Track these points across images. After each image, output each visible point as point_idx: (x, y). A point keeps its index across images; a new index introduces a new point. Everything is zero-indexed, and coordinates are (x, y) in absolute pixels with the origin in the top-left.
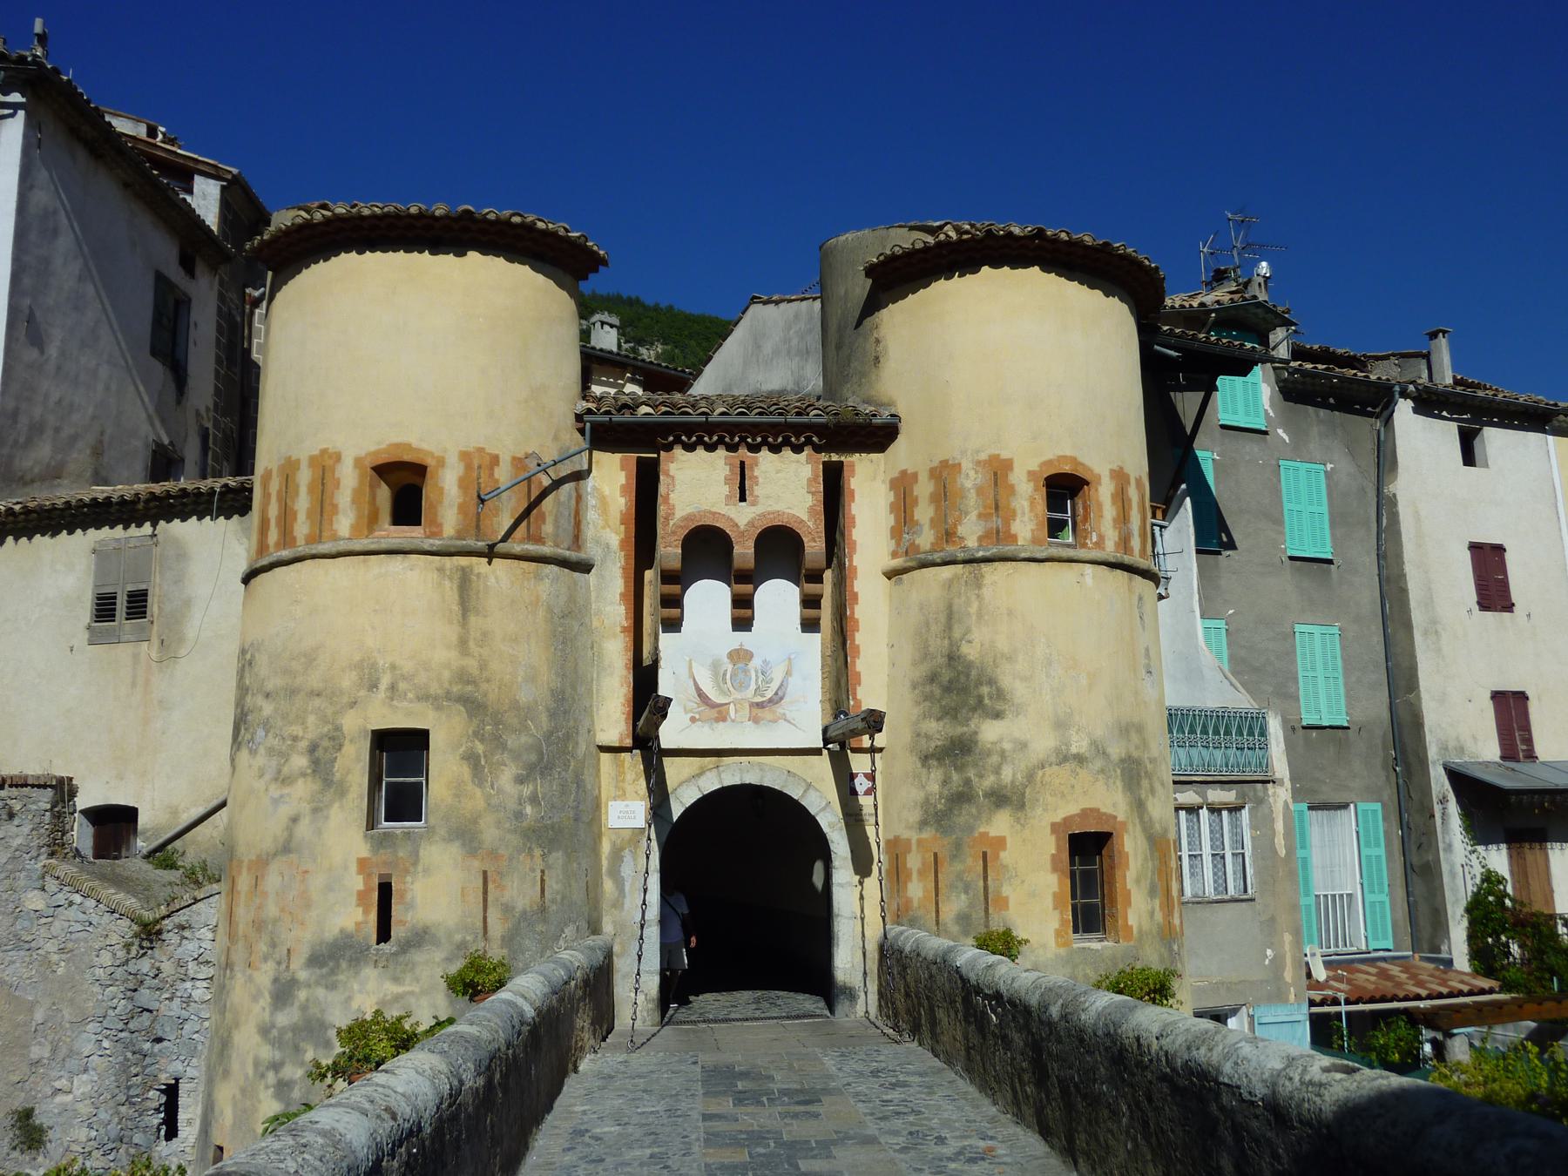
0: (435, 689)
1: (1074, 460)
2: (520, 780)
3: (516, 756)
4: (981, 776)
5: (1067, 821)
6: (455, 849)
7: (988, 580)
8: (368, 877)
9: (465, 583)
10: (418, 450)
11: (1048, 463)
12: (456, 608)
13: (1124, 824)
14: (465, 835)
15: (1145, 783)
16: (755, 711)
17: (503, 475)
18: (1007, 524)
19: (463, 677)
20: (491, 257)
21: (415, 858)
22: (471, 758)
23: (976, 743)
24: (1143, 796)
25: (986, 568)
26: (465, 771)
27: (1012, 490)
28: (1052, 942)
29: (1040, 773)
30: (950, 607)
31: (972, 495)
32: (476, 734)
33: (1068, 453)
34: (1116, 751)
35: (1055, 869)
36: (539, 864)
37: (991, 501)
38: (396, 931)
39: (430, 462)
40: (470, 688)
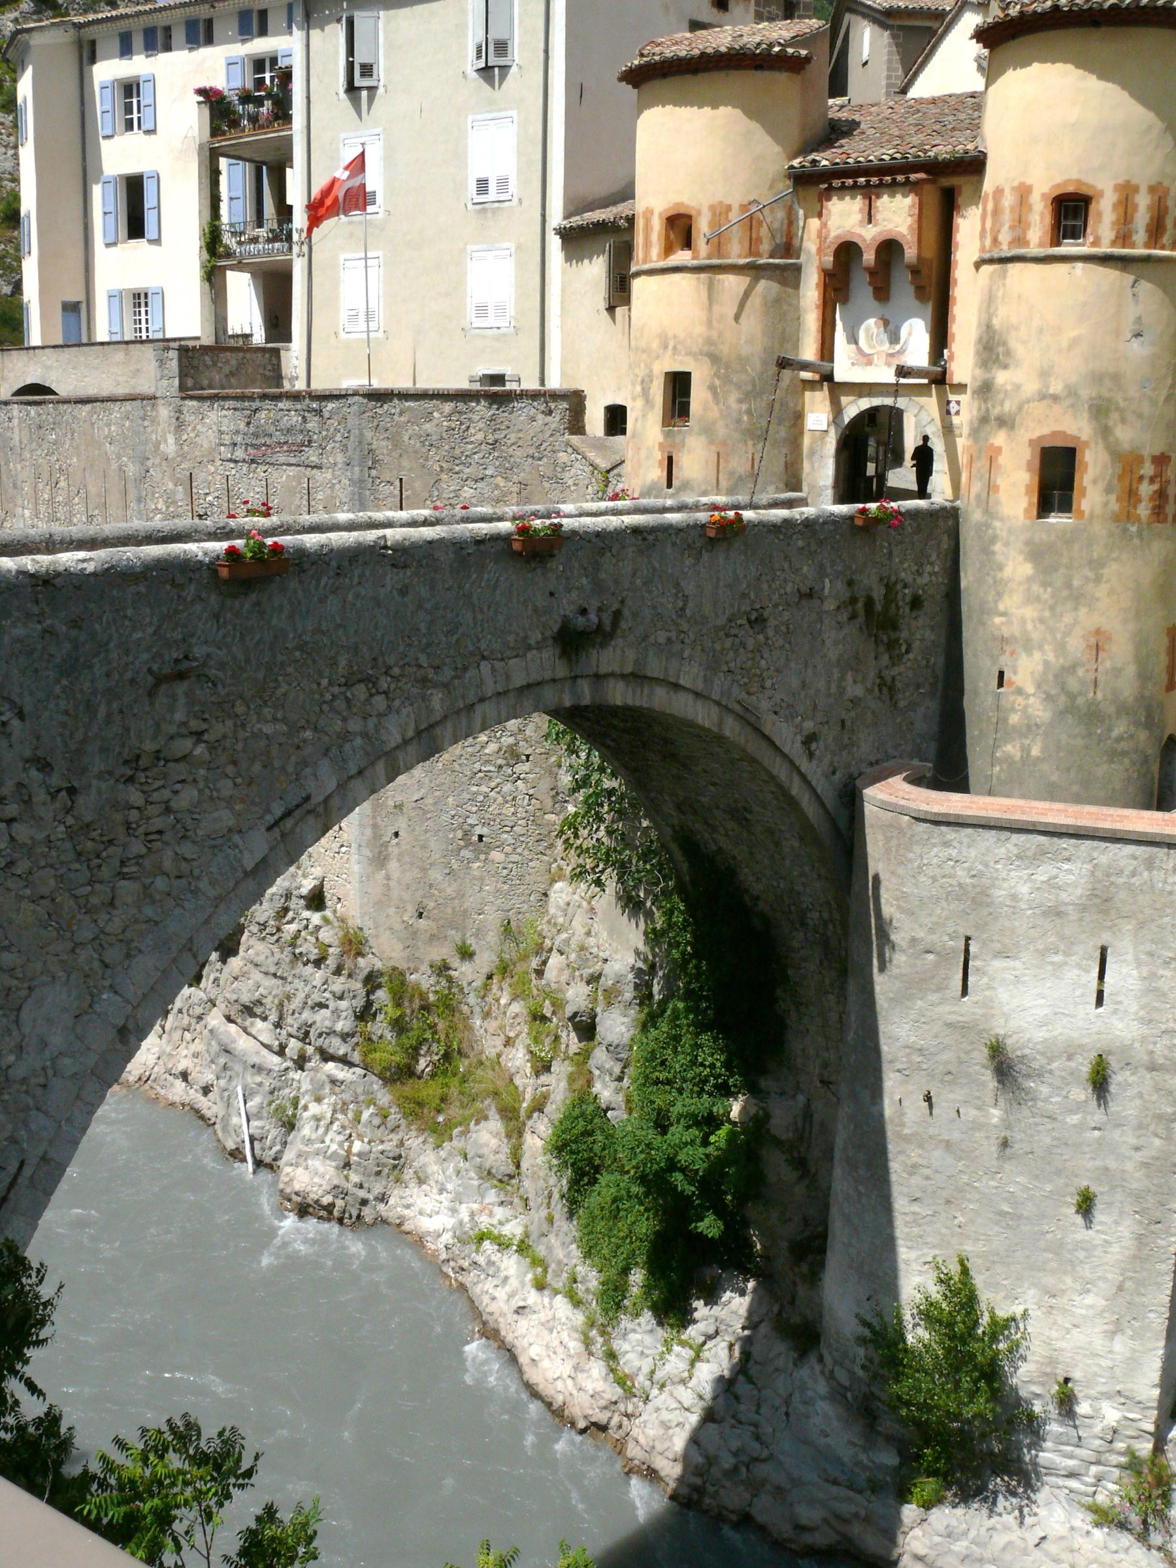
0: (695, 349)
1: (1079, 182)
2: (740, 401)
3: (738, 387)
4: (994, 407)
5: (1041, 438)
6: (703, 439)
7: (1009, 274)
8: (663, 452)
9: (711, 287)
10: (687, 207)
11: (1059, 185)
12: (706, 301)
13: (1086, 444)
14: (707, 430)
15: (1115, 416)
16: (890, 359)
17: (734, 216)
18: (1024, 232)
19: (709, 342)
20: (669, 108)
21: (683, 443)
22: (712, 388)
23: (993, 384)
24: (1111, 423)
25: (1010, 266)
26: (709, 396)
27: (1030, 208)
28: (1021, 516)
29: (1026, 406)
30: (990, 291)
31: (1007, 211)
32: (715, 375)
33: (1075, 176)
34: (1085, 393)
35: (1029, 469)
36: (751, 450)
37: (1017, 217)
38: (675, 482)
39: (693, 213)
40: (713, 348)
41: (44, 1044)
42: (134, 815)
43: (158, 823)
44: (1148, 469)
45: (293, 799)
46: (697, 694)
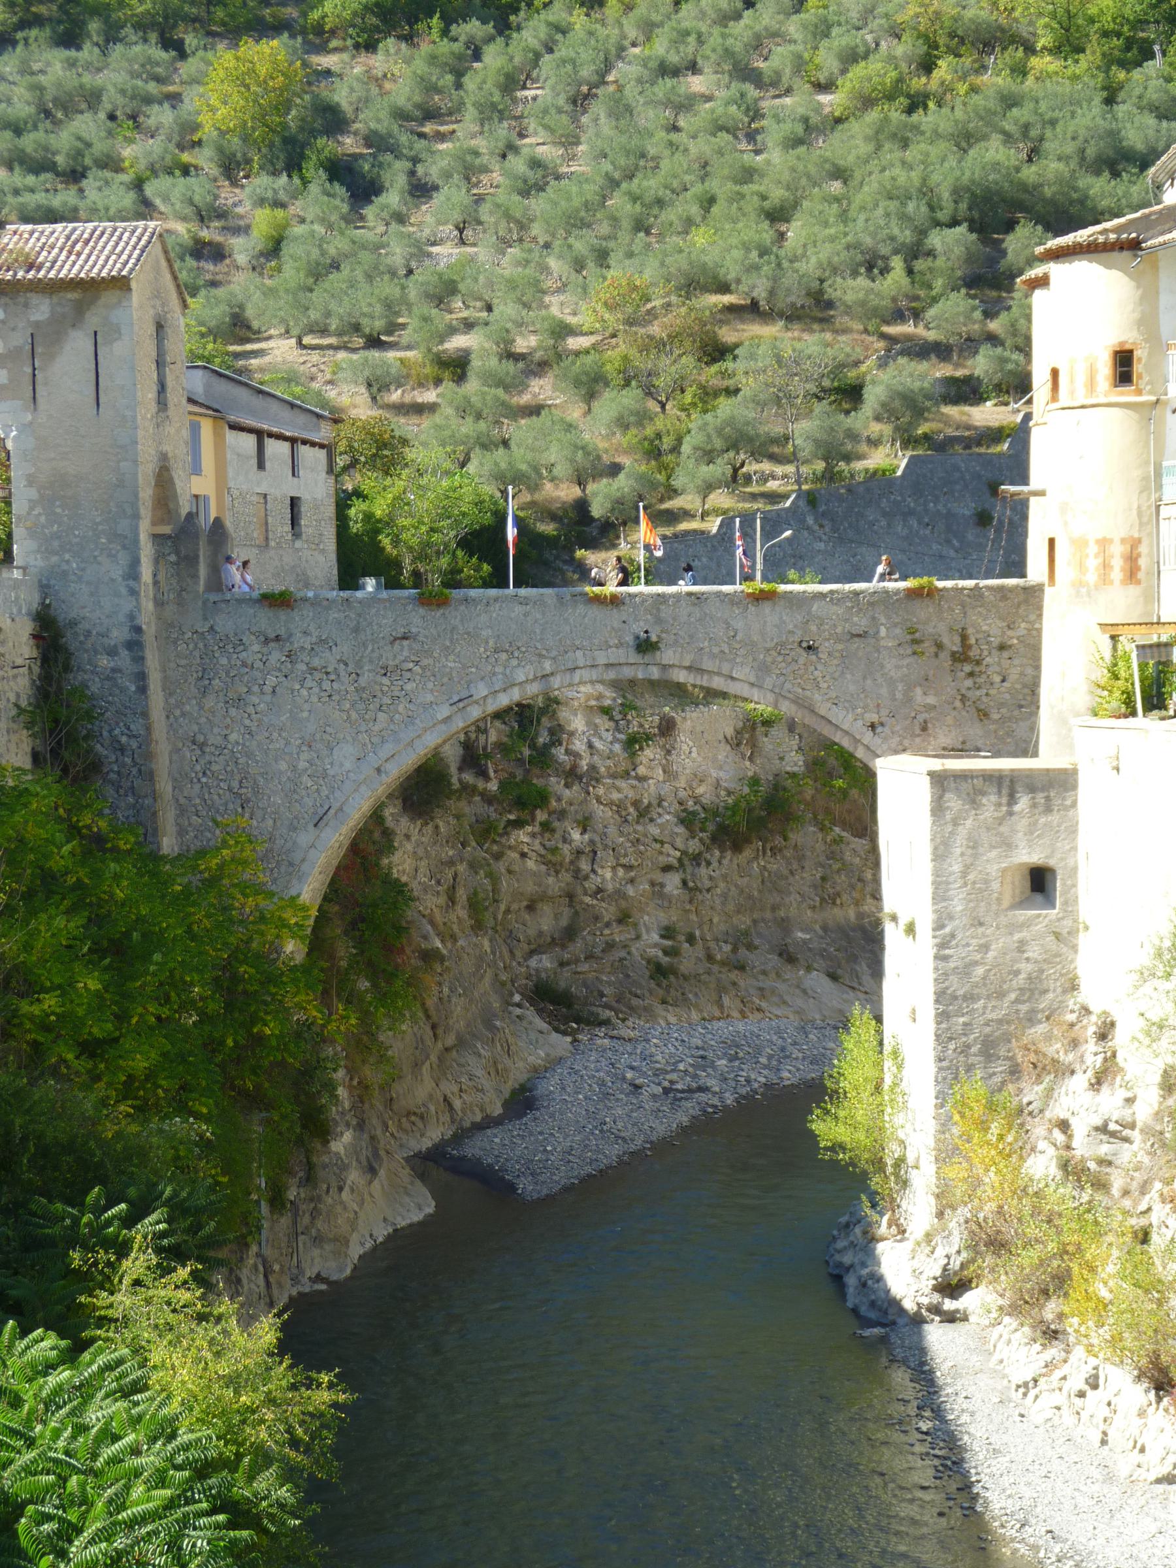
41: (341, 765)
42: (385, 689)
43: (397, 693)
44: (1093, 549)
45: (464, 694)
46: (752, 685)
